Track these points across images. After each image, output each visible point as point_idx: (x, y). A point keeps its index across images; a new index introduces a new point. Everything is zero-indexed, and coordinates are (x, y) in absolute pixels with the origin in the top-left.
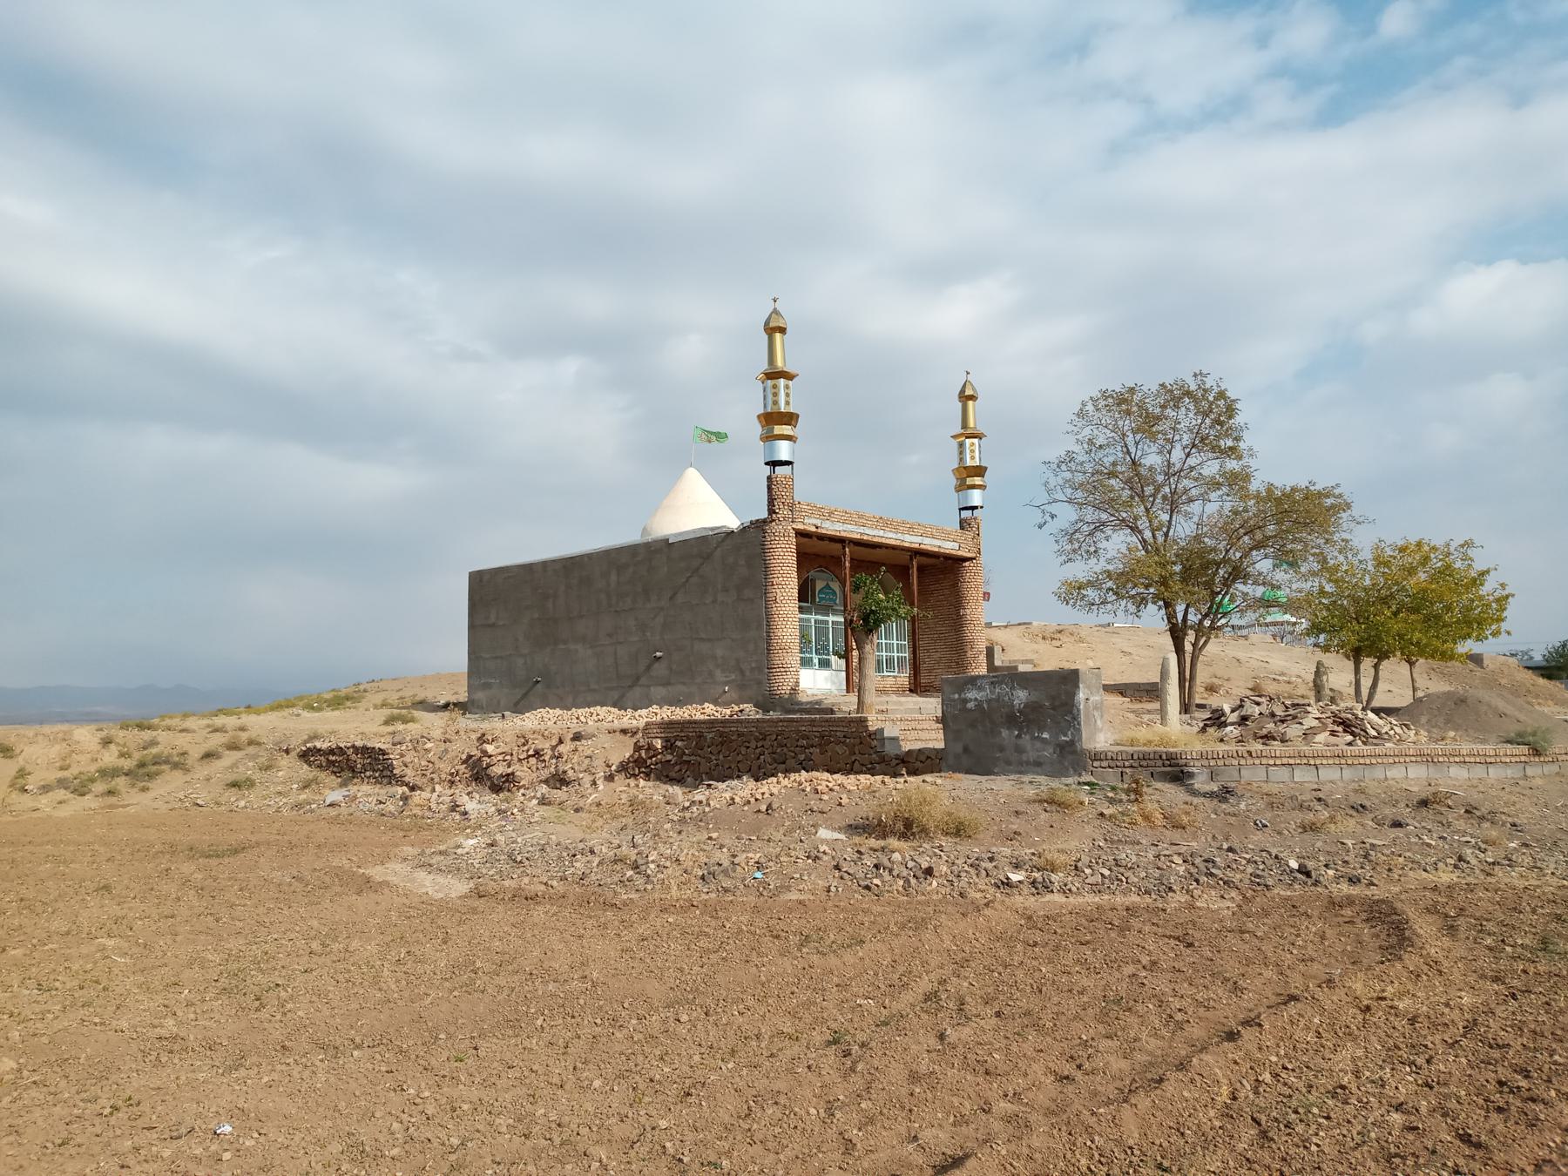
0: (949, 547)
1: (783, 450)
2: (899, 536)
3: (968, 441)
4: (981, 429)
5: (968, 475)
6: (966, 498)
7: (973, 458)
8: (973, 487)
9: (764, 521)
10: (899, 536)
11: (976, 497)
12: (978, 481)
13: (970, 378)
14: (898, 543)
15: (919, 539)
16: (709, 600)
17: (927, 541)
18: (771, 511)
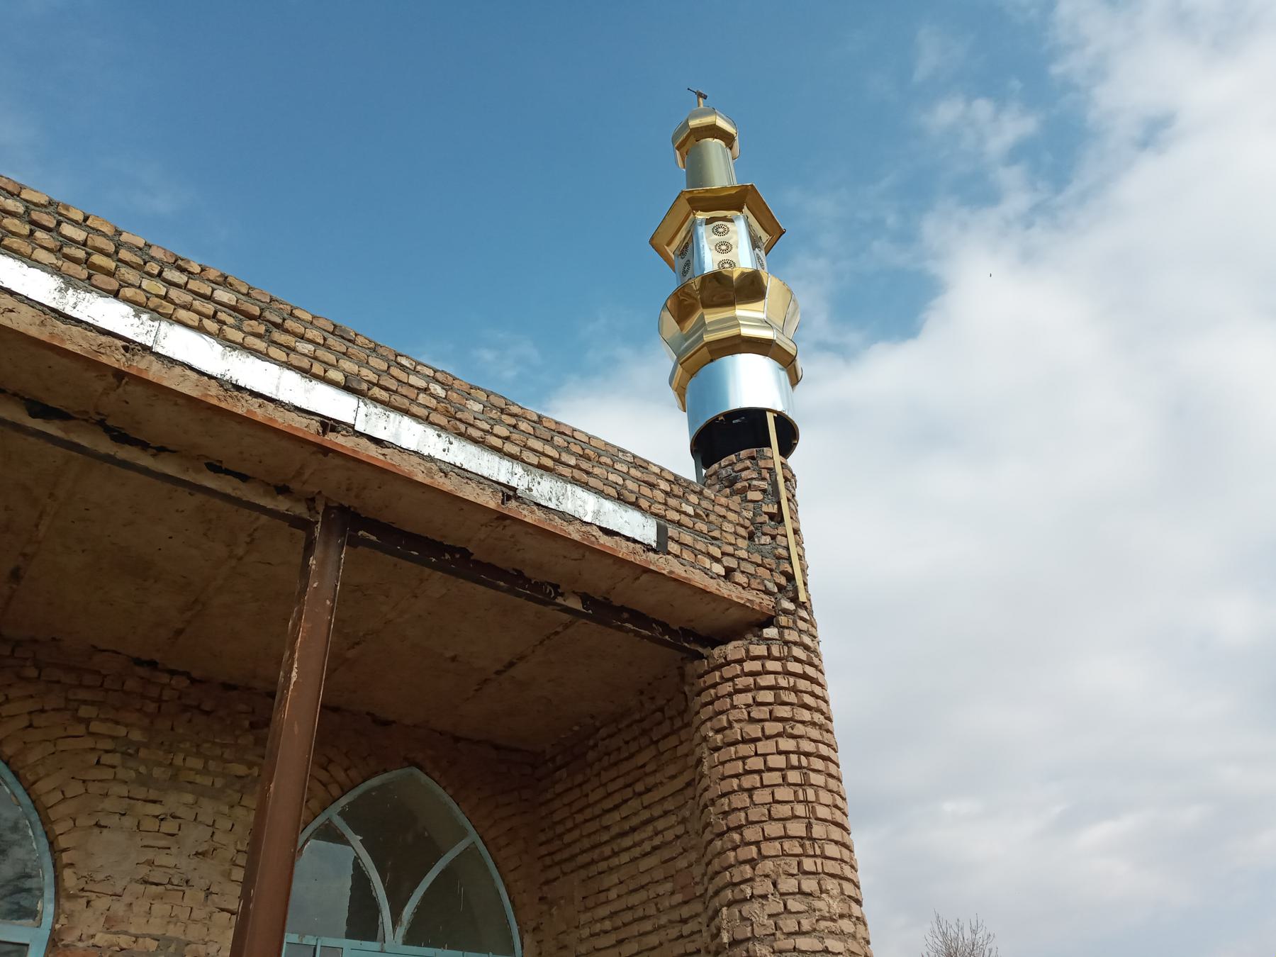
15: (338, 405)
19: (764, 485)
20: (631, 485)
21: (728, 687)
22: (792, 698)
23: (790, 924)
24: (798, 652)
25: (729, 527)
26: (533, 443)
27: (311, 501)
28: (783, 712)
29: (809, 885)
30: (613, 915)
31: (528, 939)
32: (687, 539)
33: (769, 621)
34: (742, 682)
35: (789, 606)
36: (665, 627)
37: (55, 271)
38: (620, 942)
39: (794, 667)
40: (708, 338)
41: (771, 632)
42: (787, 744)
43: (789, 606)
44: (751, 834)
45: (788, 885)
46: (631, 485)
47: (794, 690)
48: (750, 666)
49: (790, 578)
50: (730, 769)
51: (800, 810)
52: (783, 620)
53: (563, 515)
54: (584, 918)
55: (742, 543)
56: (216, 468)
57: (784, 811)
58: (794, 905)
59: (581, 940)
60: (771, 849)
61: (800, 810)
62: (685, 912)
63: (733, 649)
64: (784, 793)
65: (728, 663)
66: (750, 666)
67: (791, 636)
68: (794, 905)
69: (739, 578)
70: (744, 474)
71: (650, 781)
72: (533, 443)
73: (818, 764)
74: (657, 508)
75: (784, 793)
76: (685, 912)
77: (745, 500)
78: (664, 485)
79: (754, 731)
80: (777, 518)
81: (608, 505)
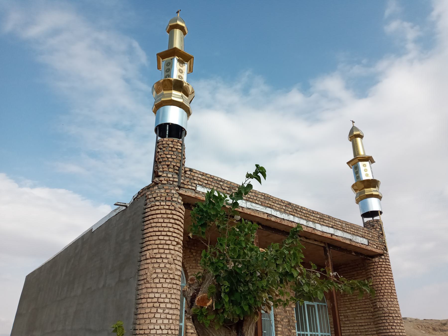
0: (361, 241)
1: (174, 115)
2: (311, 224)
3: (361, 164)
4: (368, 154)
5: (365, 188)
6: (366, 205)
7: (367, 175)
8: (372, 196)
9: (148, 188)
10: (311, 224)
11: (373, 204)
12: (372, 191)
13: (355, 125)
14: (310, 230)
15: (331, 231)
16: (101, 286)
17: (339, 233)
18: (156, 174)
19: (379, 227)
20: (363, 234)
21: (376, 266)
22: (387, 269)
23: (390, 306)
24: (388, 261)
25: (376, 238)
26: (352, 230)
27: (325, 243)
28: (386, 271)
29: (392, 300)
30: (348, 299)
31: (328, 301)
32: (371, 242)
33: (382, 255)
34: (379, 266)
35: (385, 252)
36: (364, 255)
37: (305, 219)
38: (351, 304)
39: (387, 263)
40: (366, 194)
41: (383, 257)
42: (387, 277)
43: (385, 252)
44: (382, 291)
45: (389, 300)
46: (363, 234)
47: (387, 267)
48: (380, 263)
49: (385, 246)
50: (378, 280)
51: (390, 288)
52: (385, 255)
53: (357, 242)
54: (341, 299)
55: (378, 241)
56: (315, 240)
57: (387, 288)
58: (390, 303)
59: (341, 302)
60: (386, 294)
61: (390, 288)
62: (366, 301)
63: (377, 259)
64: (387, 285)
65: (376, 262)
66: (380, 263)
67: (386, 258)
68: (390, 303)
69: (379, 248)
70: (376, 225)
71: (356, 277)
72: (352, 230)
73: (392, 280)
74: (367, 237)
75: (387, 285)
76: (366, 301)
77: (376, 230)
78: (367, 232)
79: (382, 274)
80: (382, 234)
81: (362, 239)
